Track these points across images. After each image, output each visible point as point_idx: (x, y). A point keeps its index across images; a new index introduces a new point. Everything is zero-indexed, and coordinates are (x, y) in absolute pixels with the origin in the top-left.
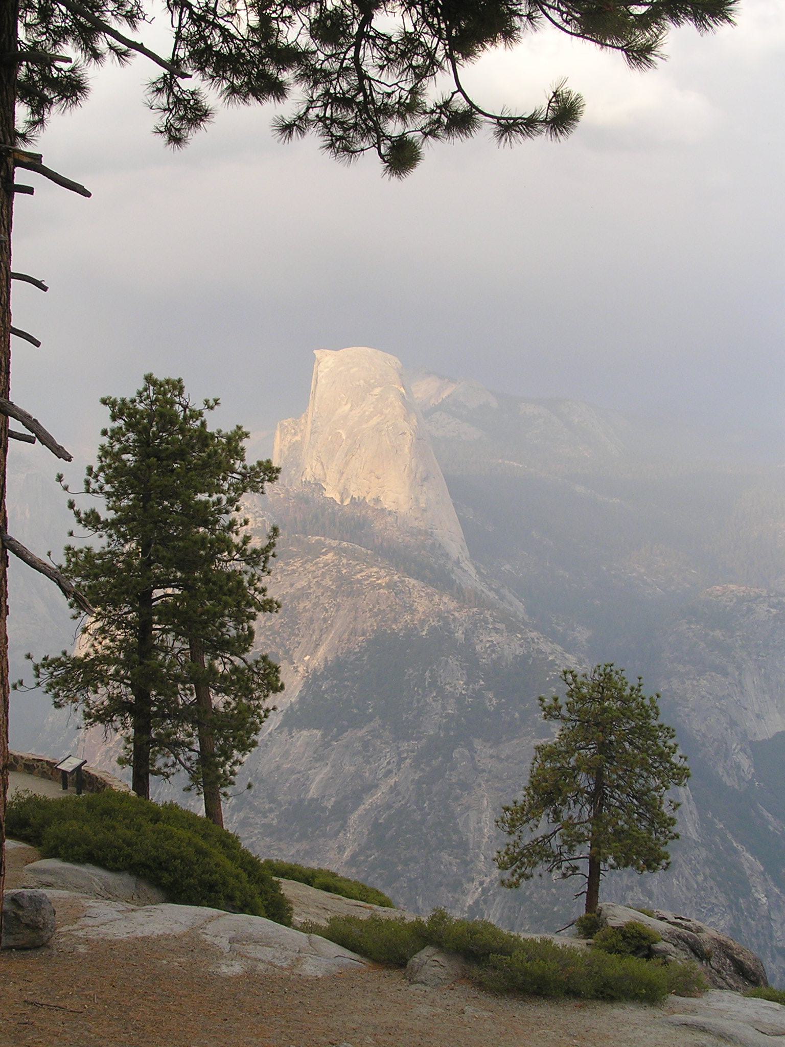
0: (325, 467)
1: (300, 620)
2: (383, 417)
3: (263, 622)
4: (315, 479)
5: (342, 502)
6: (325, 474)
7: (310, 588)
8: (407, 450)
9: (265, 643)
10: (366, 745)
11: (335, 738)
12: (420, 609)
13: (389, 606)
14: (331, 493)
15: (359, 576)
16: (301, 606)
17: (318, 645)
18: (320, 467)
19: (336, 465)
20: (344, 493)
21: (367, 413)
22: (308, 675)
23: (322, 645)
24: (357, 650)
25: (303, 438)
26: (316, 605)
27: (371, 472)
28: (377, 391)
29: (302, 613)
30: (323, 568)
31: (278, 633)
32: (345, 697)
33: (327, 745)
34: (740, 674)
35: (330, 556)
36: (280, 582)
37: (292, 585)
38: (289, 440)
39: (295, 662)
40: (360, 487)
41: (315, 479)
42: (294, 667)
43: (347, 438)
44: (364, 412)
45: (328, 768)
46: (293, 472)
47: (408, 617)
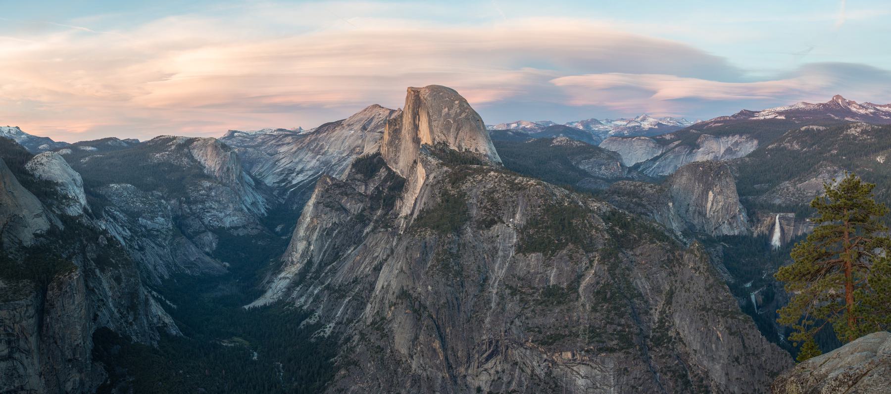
2: (467, 113)
3: (479, 204)
4: (444, 141)
8: (482, 128)
10: (571, 257)
11: (551, 255)
12: (556, 193)
13: (545, 193)
14: (453, 147)
15: (516, 181)
20: (460, 147)
21: (458, 112)
23: (516, 213)
24: (540, 214)
26: (504, 195)
27: (470, 137)
28: (457, 102)
32: (545, 236)
33: (550, 259)
35: (492, 173)
37: (485, 187)
41: (444, 141)
43: (454, 123)
44: (456, 111)
45: (555, 269)
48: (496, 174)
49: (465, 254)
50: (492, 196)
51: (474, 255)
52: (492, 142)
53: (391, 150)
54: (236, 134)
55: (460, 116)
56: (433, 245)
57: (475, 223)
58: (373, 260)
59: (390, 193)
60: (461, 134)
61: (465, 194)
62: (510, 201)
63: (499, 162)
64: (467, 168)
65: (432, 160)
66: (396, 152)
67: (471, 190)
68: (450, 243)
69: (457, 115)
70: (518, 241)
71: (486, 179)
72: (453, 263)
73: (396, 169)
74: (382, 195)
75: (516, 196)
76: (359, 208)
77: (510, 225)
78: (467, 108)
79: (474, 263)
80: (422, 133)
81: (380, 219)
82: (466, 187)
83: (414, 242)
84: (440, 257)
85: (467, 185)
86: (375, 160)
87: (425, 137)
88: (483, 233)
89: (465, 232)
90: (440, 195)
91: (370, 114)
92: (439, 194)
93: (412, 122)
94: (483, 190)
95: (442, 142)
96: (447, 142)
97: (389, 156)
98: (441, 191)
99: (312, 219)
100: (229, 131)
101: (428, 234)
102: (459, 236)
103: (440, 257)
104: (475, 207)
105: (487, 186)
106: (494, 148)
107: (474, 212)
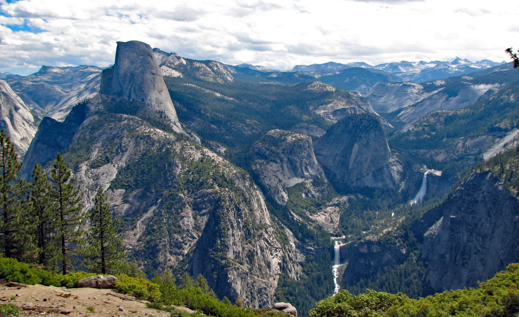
5: (129, 100)
6: (122, 90)
7: (119, 134)
15: (137, 129)
16: (115, 142)
18: (120, 87)
25: (113, 76)
28: (141, 57)
31: (106, 152)
34: (282, 163)
35: (126, 121)
37: (111, 134)
43: (130, 76)
46: (109, 89)
47: (158, 145)
54: (48, 70)
55: (138, 69)
60: (134, 85)
61: (95, 138)
69: (136, 68)
71: (116, 127)
77: (116, 166)
78: (148, 63)
89: (80, 169)
99: (32, 154)
100: (43, 66)
102: (74, 173)
104: (97, 150)
107: (95, 154)
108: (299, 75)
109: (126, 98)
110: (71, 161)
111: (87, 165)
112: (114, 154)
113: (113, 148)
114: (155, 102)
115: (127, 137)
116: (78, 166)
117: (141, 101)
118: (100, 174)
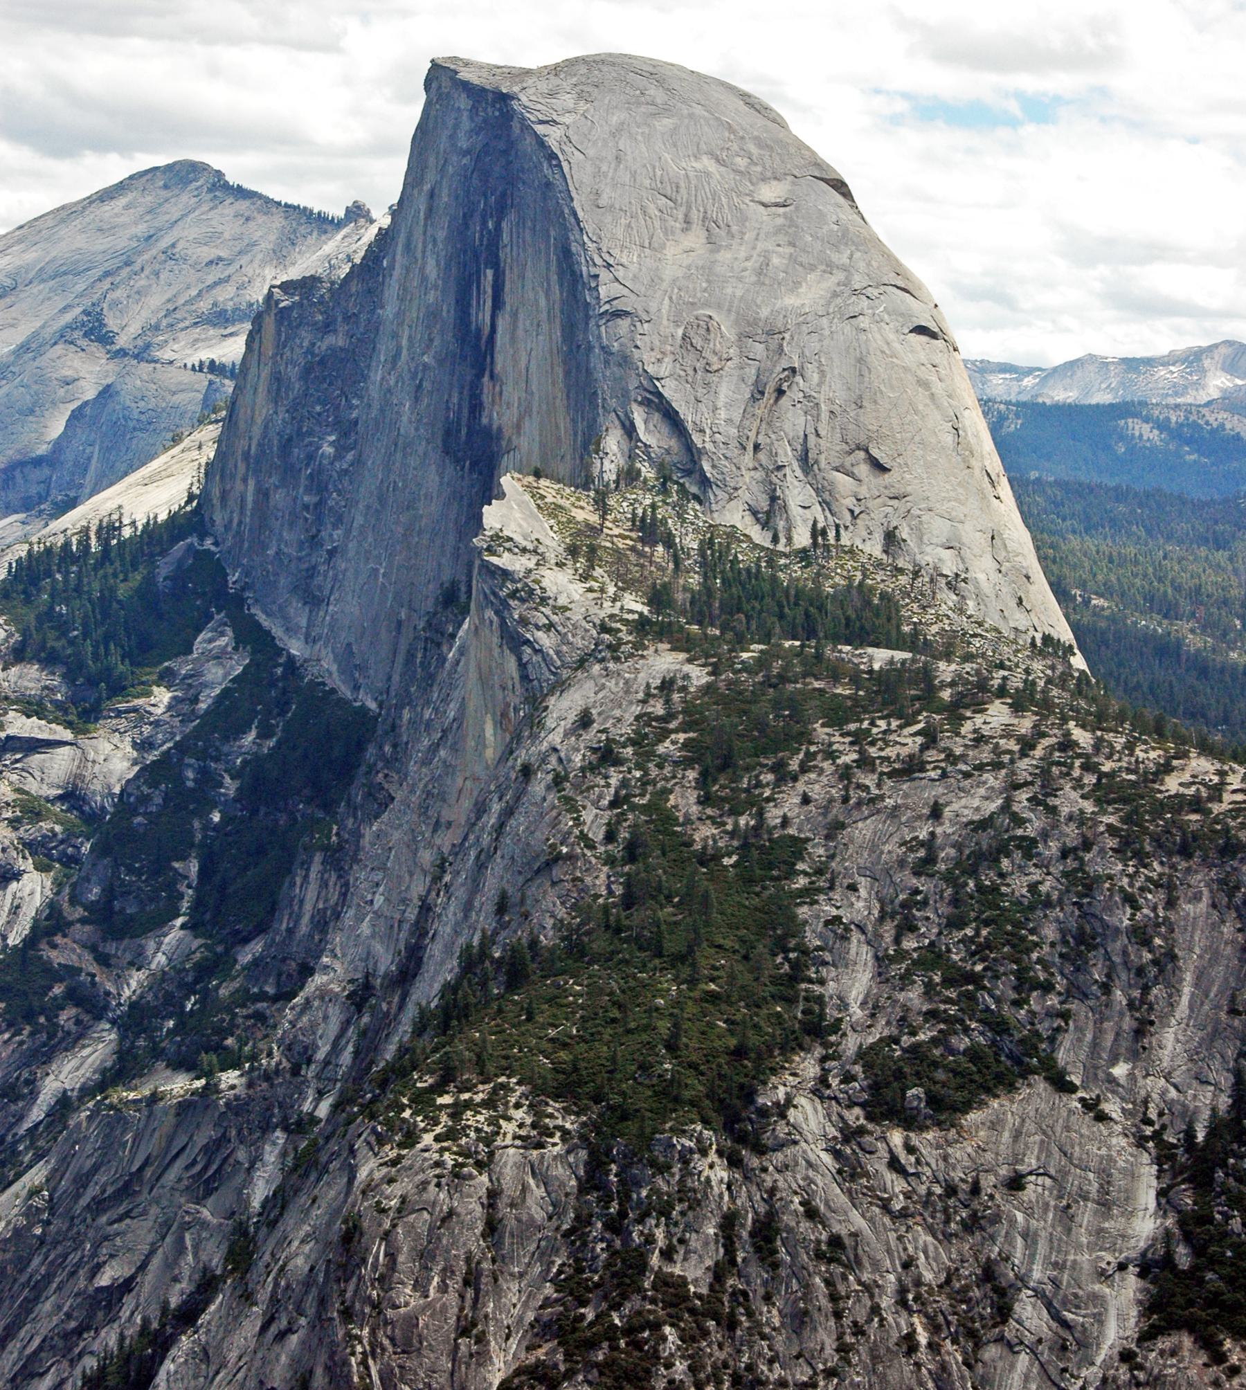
0: (690, 427)
1: (1033, 931)
3: (888, 938)
7: (1019, 821)
9: (932, 1015)
16: (1018, 886)
17: (1152, 1023)
18: (665, 429)
19: (729, 421)
22: (1157, 1136)
29: (1032, 908)
30: (1023, 754)
35: (998, 715)
36: (882, 798)
37: (936, 813)
38: (306, 344)
39: (1077, 1082)
40: (826, 496)
42: (1082, 1100)
43: (743, 336)
48: (1025, 725)
49: (768, 1298)
50: (988, 878)
51: (838, 1315)
52: (1005, 490)
53: (279, 498)
56: (539, 1215)
57: (858, 1069)
58: (91, 1316)
59: (255, 812)
60: (793, 420)
61: (797, 847)
62: (1117, 931)
63: (1047, 639)
64: (816, 664)
65: (576, 590)
66: (319, 519)
67: (842, 826)
68: (665, 1212)
70: (1168, 1234)
71: (952, 758)
72: (680, 1366)
73: (310, 639)
74: (197, 824)
75: (1162, 895)
76: (15, 910)
77: (1112, 1107)
79: (830, 1373)
80: (512, 393)
81: (169, 997)
82: (806, 800)
83: (404, 1186)
84: (589, 1313)
85: (816, 792)
86: (164, 568)
87: (531, 427)
88: (910, 1149)
89: (782, 1130)
90: (616, 849)
91: (141, 229)
92: (610, 837)
93: (448, 312)
94: (923, 835)
95: (647, 472)
96: (688, 473)
97: (264, 547)
98: (621, 818)
101: (509, 1128)
102: (734, 1162)
103: (589, 1313)
104: (859, 951)
105: (955, 806)
106: (1019, 537)
108: (1162, 426)
109: (734, 516)
110: (672, 1047)
111: (820, 1089)
112: (1052, 1001)
113: (1021, 947)
114: (988, 563)
115: (1128, 847)
116: (749, 1095)
117: (874, 548)
118: (988, 1182)
